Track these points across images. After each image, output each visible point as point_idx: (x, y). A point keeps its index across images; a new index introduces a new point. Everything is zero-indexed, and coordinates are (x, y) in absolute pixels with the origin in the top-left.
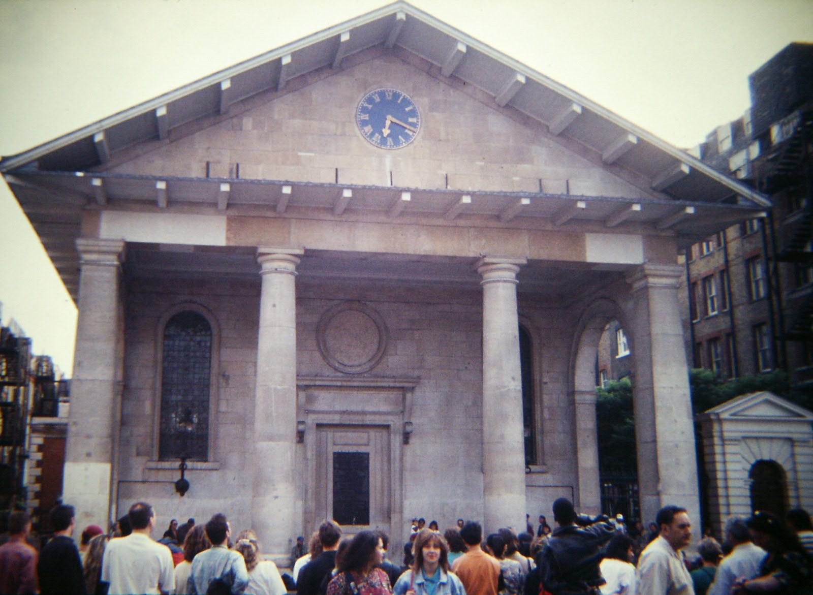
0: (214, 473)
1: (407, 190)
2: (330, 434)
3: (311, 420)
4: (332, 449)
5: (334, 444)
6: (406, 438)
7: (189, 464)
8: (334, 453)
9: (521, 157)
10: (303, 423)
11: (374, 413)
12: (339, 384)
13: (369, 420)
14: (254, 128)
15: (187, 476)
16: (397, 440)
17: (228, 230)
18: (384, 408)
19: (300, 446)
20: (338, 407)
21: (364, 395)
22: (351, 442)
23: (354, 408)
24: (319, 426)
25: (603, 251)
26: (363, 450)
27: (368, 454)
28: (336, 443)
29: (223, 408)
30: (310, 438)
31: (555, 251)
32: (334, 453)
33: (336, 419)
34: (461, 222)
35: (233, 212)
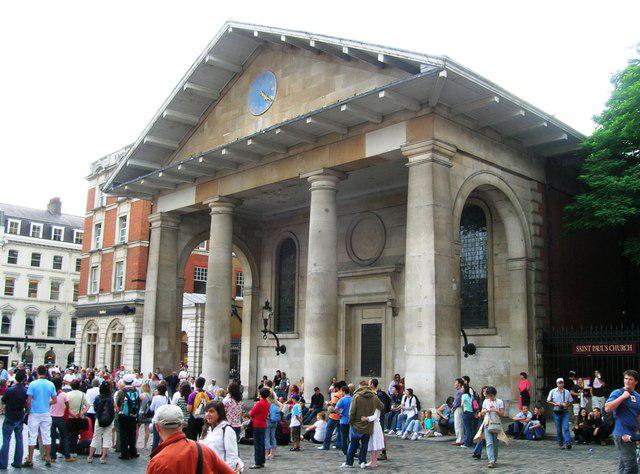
1: (222, 148)
4: (360, 322)
6: (395, 314)
7: (279, 336)
9: (328, 87)
11: (376, 294)
12: (351, 275)
13: (375, 299)
14: (209, 126)
16: (390, 312)
17: (197, 194)
18: (382, 289)
20: (358, 291)
21: (370, 281)
23: (365, 291)
24: (350, 306)
25: (379, 145)
26: (378, 321)
31: (346, 156)
34: (291, 153)
35: (197, 183)
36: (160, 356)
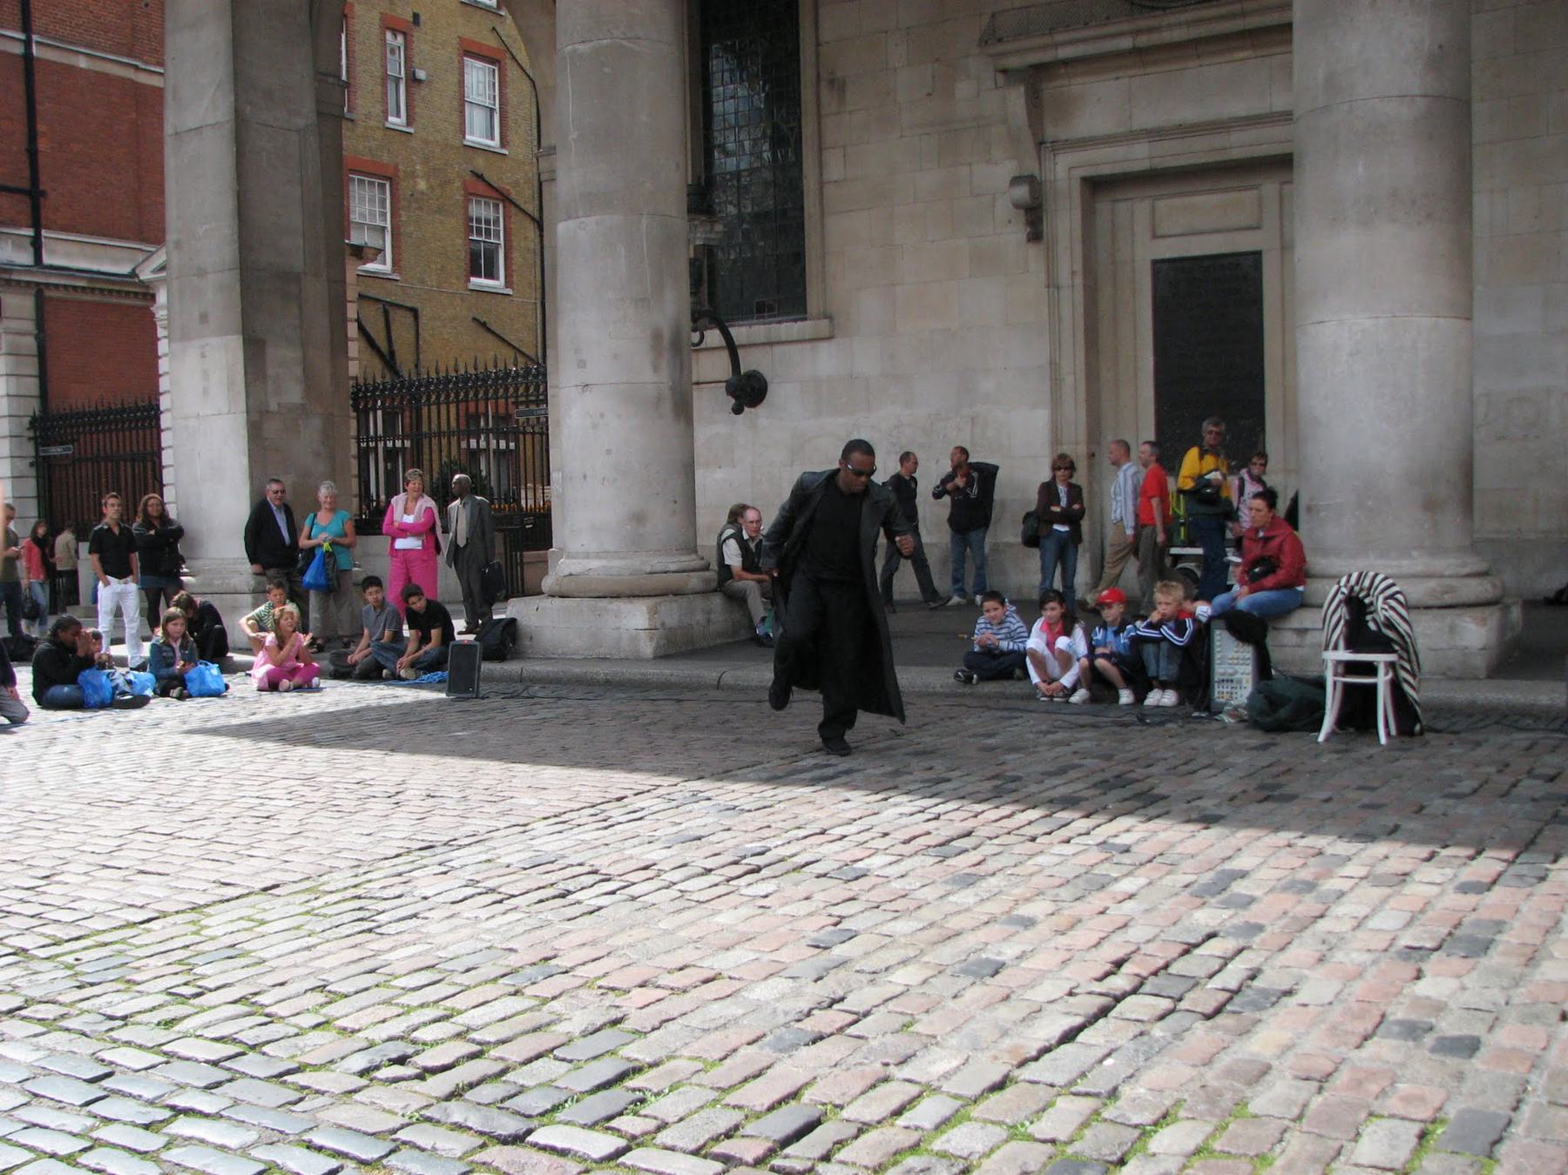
0: (824, 345)
2: (1135, 211)
3: (1064, 171)
5: (1155, 236)
7: (739, 333)
8: (1155, 263)
10: (1032, 181)
15: (749, 362)
19: (1034, 252)
22: (1199, 226)
23: (1189, 113)
24: (1096, 186)
27: (1256, 256)
28: (1159, 232)
29: (834, 170)
30: (1065, 222)
32: (1156, 263)
33: (1139, 156)
36: (272, 428)
